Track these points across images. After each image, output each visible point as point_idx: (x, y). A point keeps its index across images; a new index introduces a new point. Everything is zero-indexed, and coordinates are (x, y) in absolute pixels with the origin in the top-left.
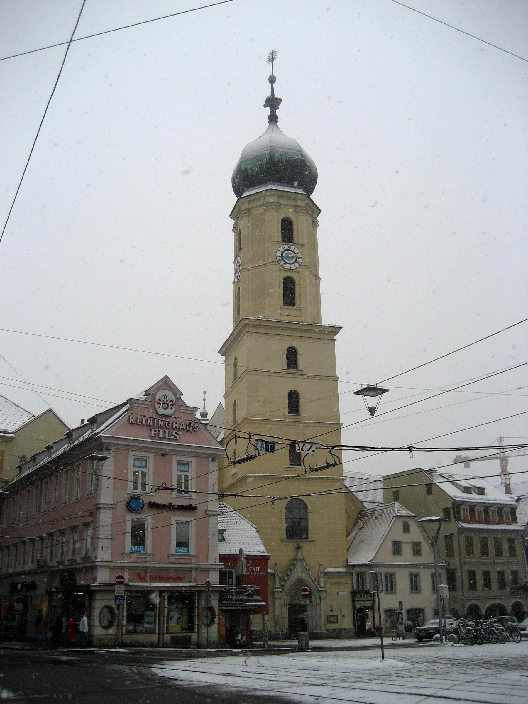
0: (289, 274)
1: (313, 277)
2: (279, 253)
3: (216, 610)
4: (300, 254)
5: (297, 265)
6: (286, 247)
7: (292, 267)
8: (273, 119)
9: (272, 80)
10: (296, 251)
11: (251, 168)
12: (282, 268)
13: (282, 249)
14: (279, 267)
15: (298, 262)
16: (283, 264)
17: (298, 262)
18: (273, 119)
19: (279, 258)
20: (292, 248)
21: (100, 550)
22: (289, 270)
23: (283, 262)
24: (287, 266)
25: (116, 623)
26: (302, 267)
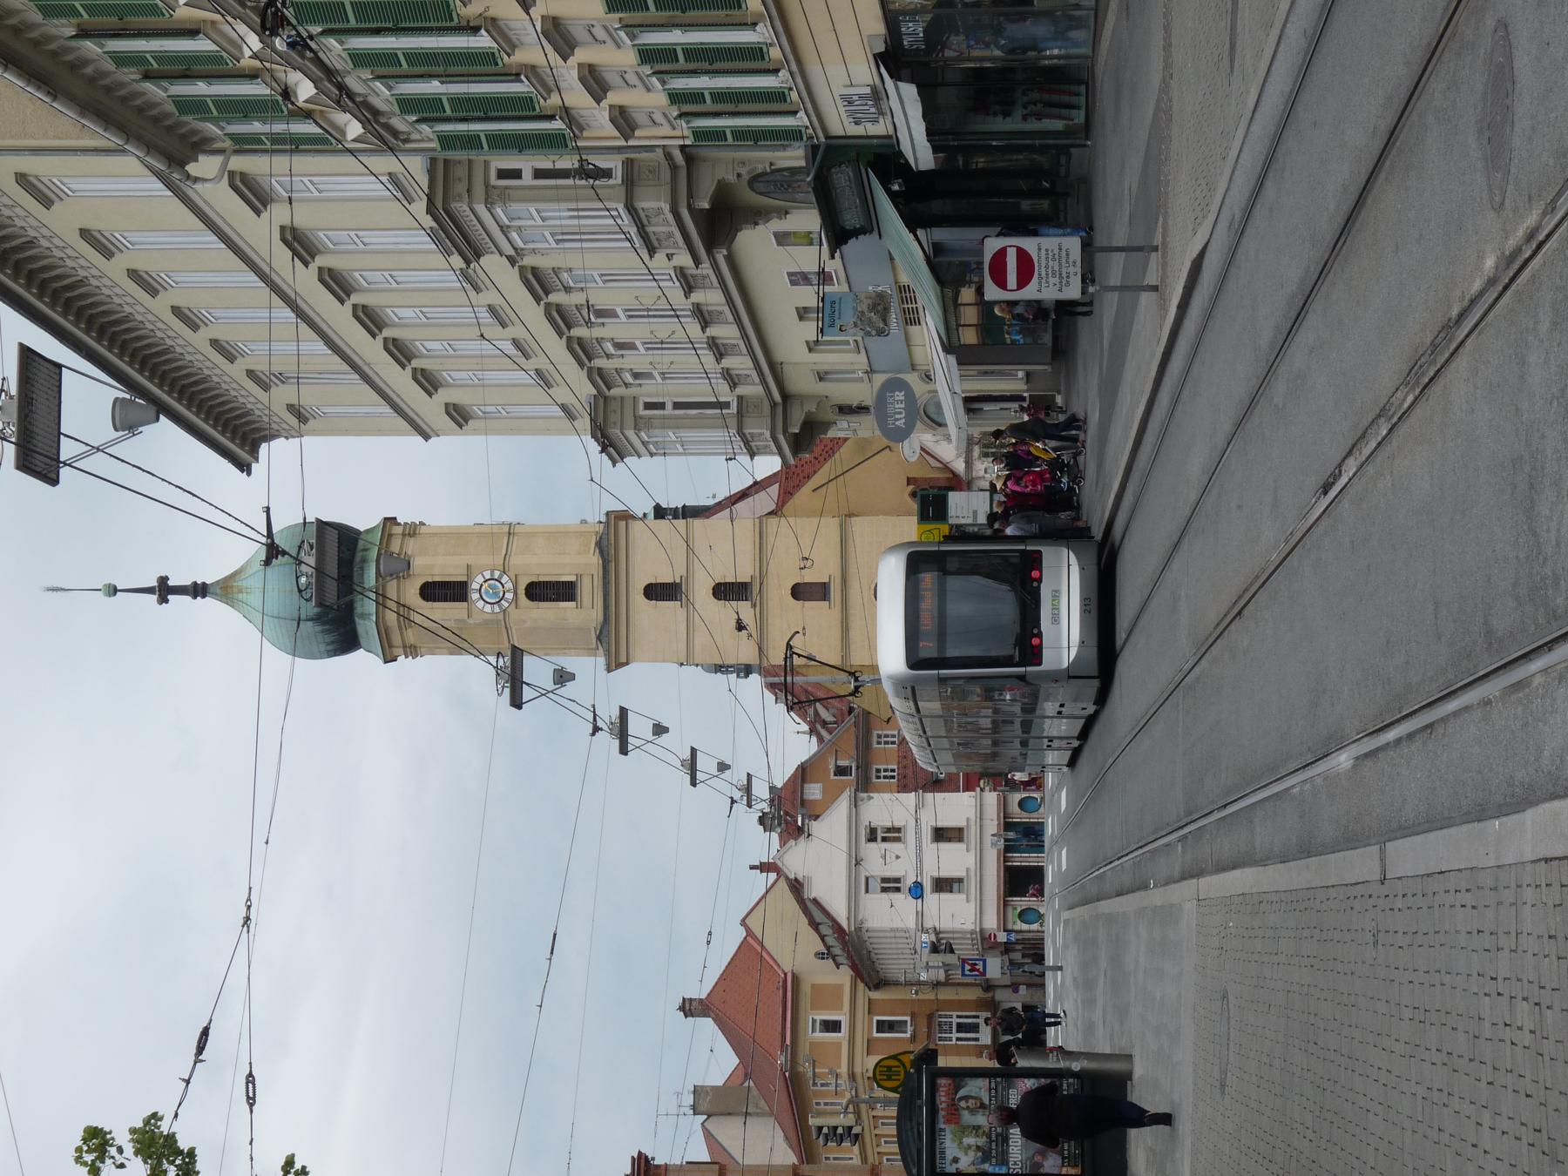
0: (522, 591)
1: (515, 542)
2: (488, 608)
3: (1024, 795)
4: (484, 573)
5: (505, 579)
6: (475, 596)
7: (509, 585)
8: (198, 590)
9: (113, 590)
10: (480, 579)
11: (328, 644)
12: (513, 605)
13: (480, 604)
14: (512, 610)
15: (501, 577)
16: (508, 602)
17: (501, 577)
18: (198, 590)
19: (497, 609)
20: (475, 586)
21: (963, 926)
22: (516, 593)
23: (503, 602)
24: (509, 596)
25: (1036, 908)
26: (506, 569)
